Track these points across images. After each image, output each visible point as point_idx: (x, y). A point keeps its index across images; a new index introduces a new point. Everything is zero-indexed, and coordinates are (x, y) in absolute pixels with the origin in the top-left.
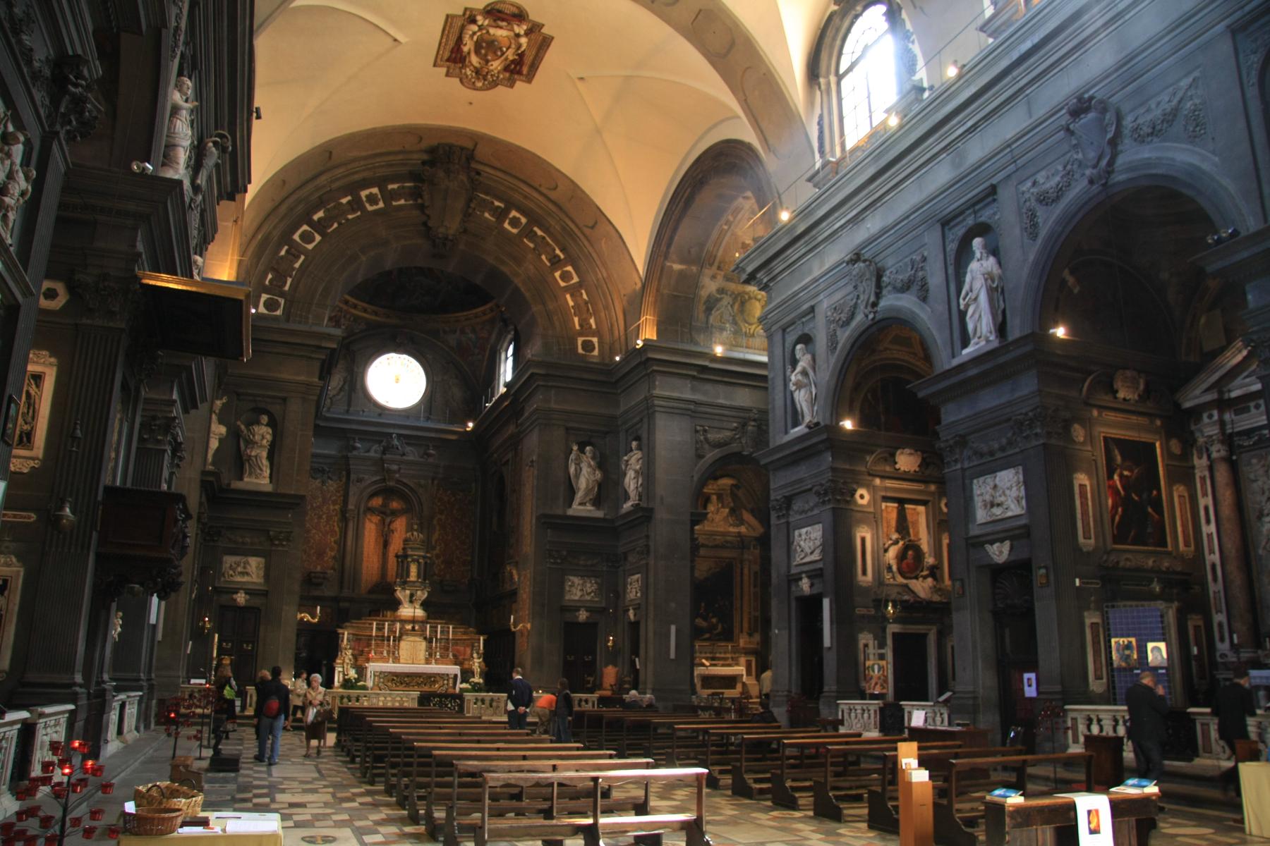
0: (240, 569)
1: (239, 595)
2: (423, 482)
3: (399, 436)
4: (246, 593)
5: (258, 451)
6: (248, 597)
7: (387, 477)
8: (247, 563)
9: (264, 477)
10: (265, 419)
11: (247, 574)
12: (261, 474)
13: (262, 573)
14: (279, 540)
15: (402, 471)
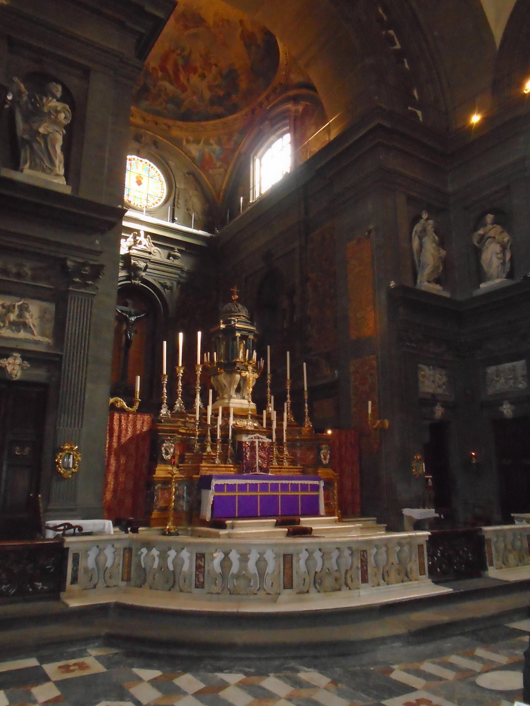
0: (13, 317)
1: (11, 360)
2: (168, 284)
3: (146, 233)
4: (23, 358)
5: (50, 130)
6: (27, 364)
7: (133, 274)
8: (23, 309)
9: (57, 175)
10: (58, 90)
11: (25, 326)
12: (52, 171)
13: (50, 327)
14: (82, 276)
15: (148, 270)
